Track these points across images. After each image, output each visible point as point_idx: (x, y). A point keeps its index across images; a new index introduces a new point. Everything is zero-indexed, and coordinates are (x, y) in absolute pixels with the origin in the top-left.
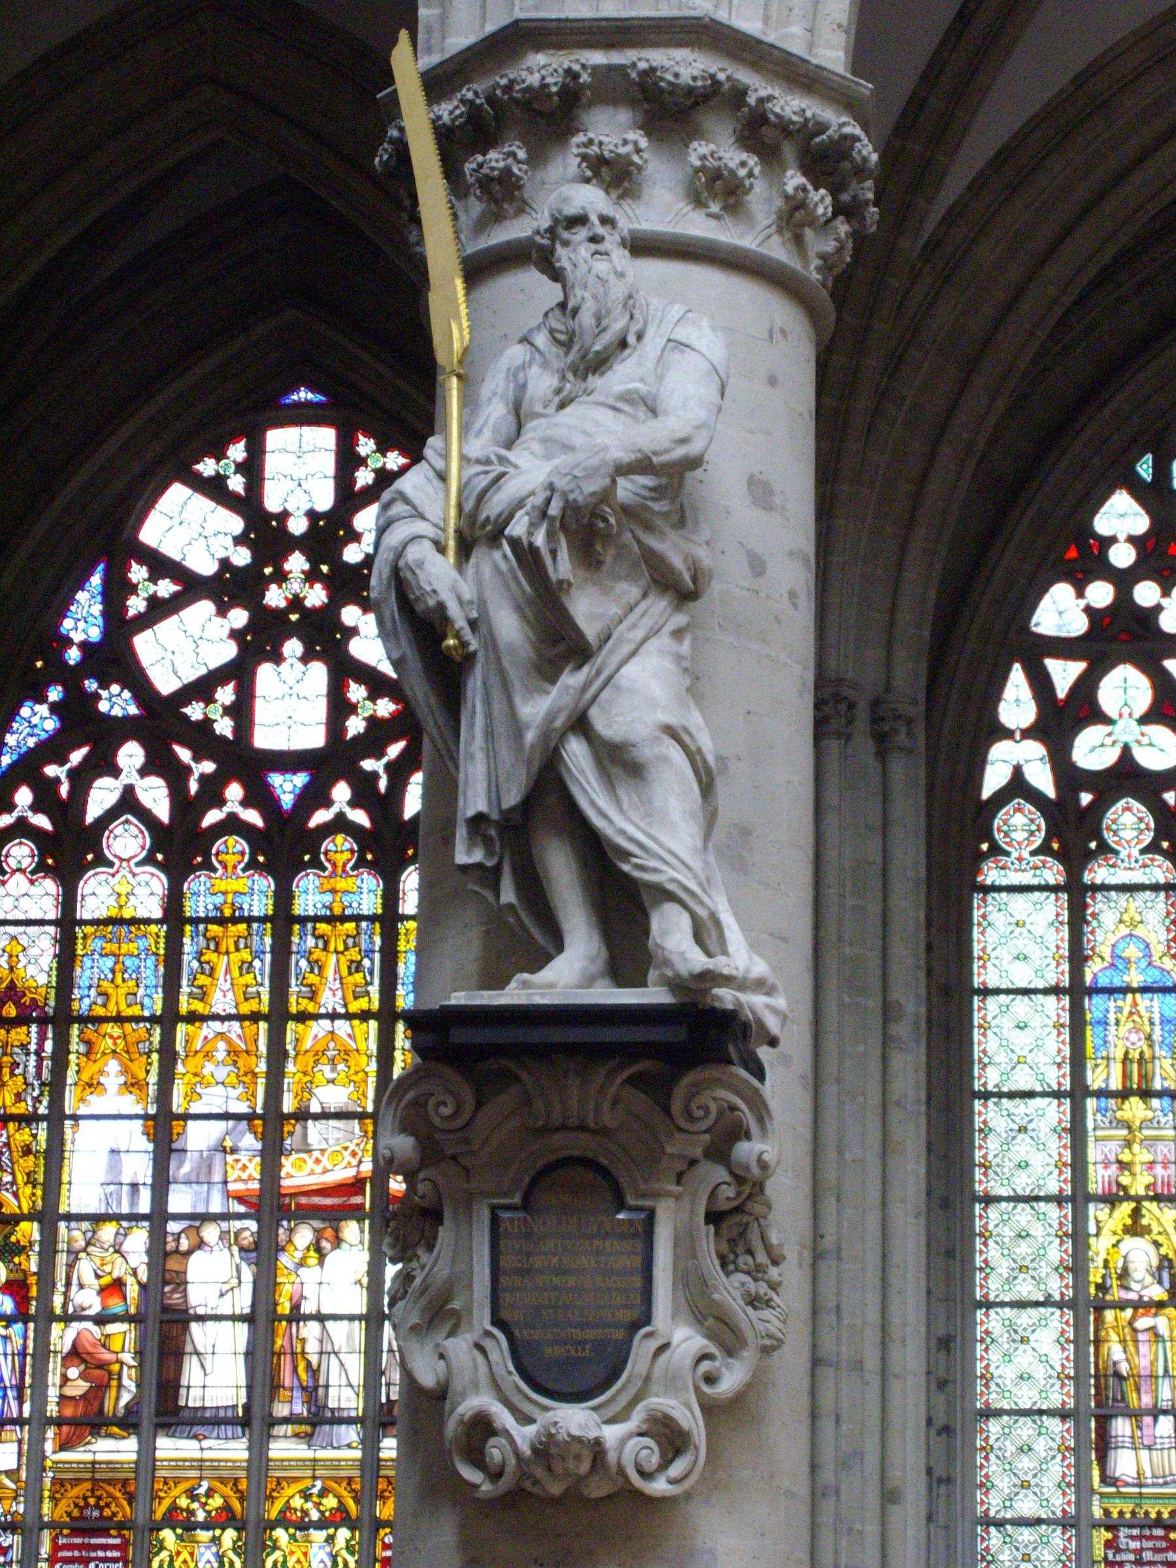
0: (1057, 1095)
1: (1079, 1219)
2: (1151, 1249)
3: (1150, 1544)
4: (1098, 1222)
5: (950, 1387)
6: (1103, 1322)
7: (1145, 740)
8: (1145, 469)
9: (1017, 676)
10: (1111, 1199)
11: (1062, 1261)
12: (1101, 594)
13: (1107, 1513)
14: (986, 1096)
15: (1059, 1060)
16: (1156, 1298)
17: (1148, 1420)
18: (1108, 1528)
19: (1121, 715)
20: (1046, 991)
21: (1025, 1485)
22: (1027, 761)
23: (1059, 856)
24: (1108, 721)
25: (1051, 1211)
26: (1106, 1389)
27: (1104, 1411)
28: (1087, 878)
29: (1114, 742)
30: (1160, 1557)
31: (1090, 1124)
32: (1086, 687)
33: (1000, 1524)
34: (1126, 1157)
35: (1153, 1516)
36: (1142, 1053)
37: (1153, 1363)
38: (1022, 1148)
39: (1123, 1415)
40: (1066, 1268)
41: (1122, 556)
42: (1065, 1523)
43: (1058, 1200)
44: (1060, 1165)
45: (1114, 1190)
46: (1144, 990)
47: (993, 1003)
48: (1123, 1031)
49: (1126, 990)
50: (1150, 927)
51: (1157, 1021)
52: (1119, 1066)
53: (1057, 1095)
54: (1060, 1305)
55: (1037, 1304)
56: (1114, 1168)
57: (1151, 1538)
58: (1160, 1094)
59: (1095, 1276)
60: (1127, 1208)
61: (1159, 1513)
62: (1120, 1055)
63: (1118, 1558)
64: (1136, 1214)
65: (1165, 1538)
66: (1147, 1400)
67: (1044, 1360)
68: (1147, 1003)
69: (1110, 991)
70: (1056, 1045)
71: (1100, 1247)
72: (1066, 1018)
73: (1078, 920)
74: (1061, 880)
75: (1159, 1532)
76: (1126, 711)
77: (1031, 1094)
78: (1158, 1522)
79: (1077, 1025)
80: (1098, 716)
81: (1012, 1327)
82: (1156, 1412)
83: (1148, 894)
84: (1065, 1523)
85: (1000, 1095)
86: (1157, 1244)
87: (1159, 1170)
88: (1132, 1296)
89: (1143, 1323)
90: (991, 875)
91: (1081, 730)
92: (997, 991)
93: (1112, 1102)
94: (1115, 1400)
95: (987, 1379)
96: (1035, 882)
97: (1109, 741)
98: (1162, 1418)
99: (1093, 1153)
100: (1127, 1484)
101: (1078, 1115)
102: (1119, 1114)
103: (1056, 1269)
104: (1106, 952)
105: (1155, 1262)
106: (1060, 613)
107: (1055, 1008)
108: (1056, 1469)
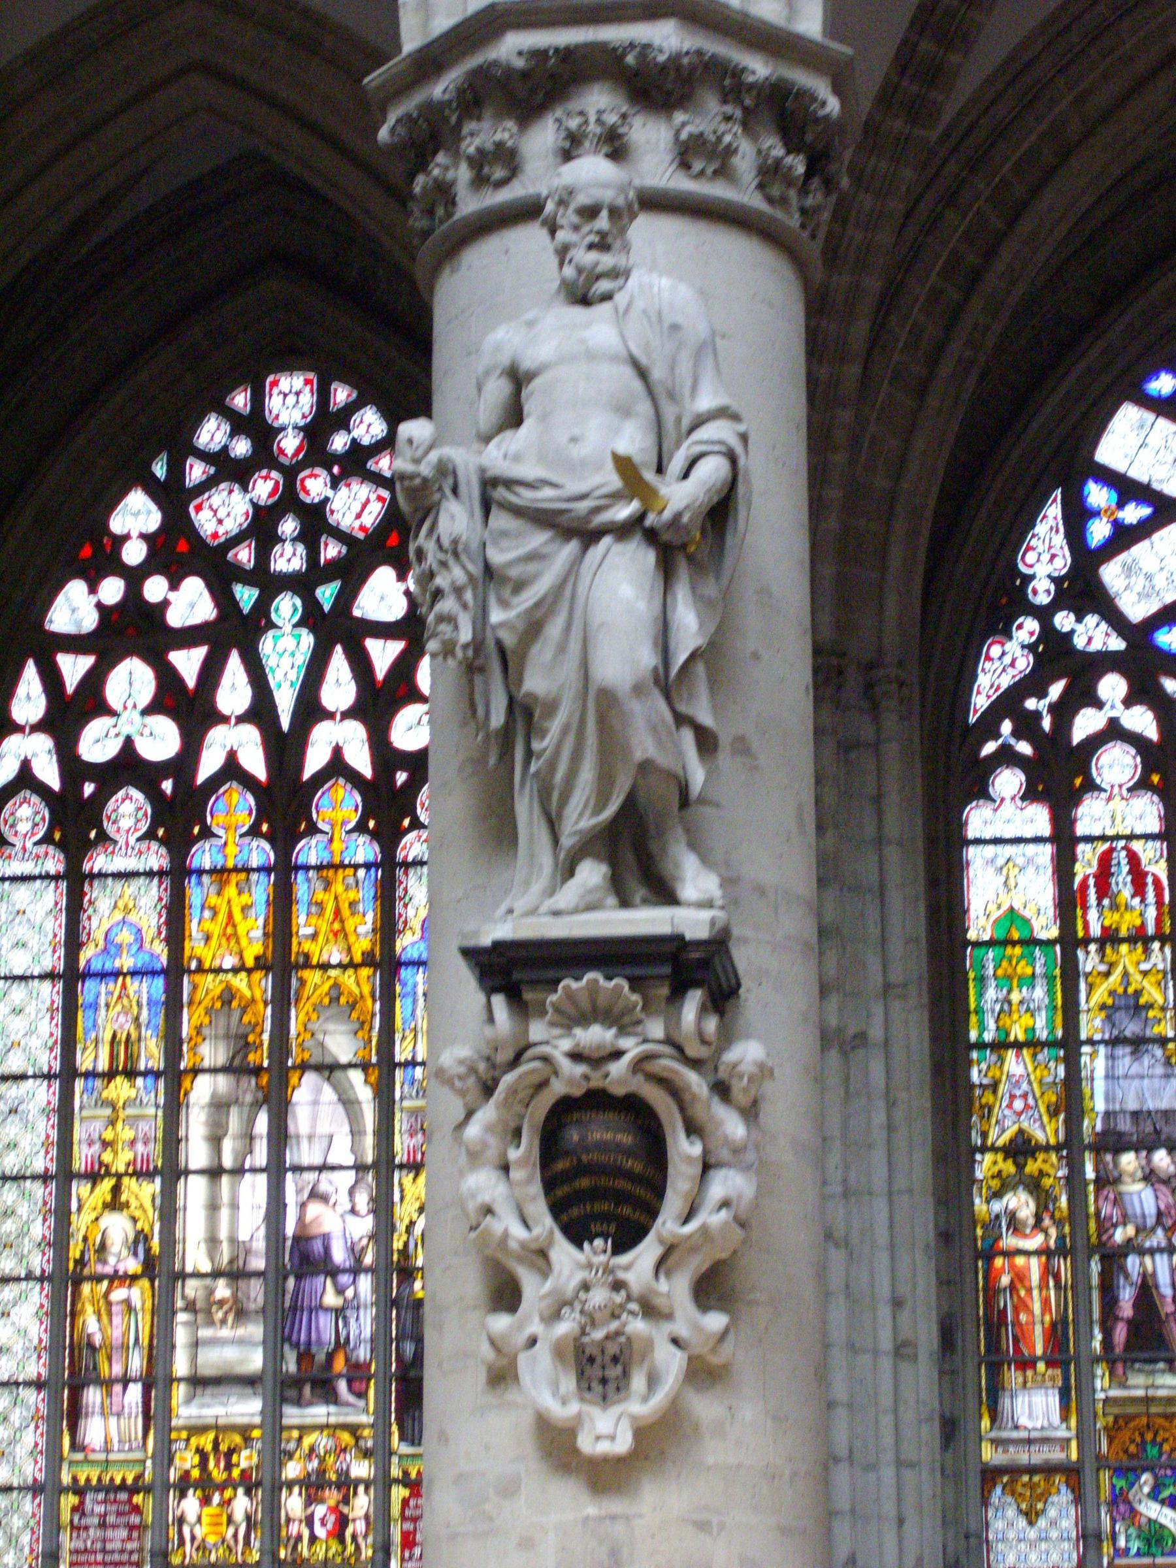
1: (64, 1196)
3: (114, 1508)
4: (79, 1200)
6: (80, 1295)
8: (160, 470)
10: (93, 1177)
11: (44, 1237)
12: (112, 590)
13: (75, 1479)
16: (130, 1272)
17: (118, 1388)
18: (76, 1493)
19: (125, 708)
20: (42, 977)
23: (62, 846)
25: (37, 1190)
27: (77, 1381)
28: (86, 867)
29: (117, 735)
30: (123, 1520)
32: (94, 681)
34: (109, 1135)
35: (118, 1481)
36: (129, 1036)
40: (49, 1244)
41: (134, 553)
43: (45, 1178)
44: (47, 1145)
45: (96, 1167)
46: (134, 973)
48: (112, 1013)
49: (116, 974)
50: (142, 912)
51: (144, 1001)
53: (48, 1076)
54: (41, 1279)
55: (18, 1279)
56: (97, 1147)
58: (146, 1074)
59: (75, 1252)
60: (107, 1184)
61: (124, 1480)
62: (108, 1036)
63: (83, 1522)
64: (116, 1190)
66: (117, 1369)
68: (136, 984)
69: (103, 975)
70: (48, 1029)
71: (80, 1223)
72: (58, 1001)
73: (75, 908)
74: (61, 868)
75: (123, 1496)
77: (23, 1077)
78: (123, 1486)
79: (70, 1010)
80: (102, 708)
82: (126, 1381)
83: (142, 880)
84: (35, 1489)
86: (135, 1220)
87: (140, 1147)
88: (108, 1270)
89: (119, 1294)
91: (88, 723)
93: (98, 1083)
96: (36, 872)
98: (131, 1386)
99: (79, 1132)
100: (93, 1451)
101: (66, 1096)
102: (105, 1094)
104: (99, 935)
105: (131, 1236)
106: (73, 611)
107: (49, 992)
108: (29, 1438)
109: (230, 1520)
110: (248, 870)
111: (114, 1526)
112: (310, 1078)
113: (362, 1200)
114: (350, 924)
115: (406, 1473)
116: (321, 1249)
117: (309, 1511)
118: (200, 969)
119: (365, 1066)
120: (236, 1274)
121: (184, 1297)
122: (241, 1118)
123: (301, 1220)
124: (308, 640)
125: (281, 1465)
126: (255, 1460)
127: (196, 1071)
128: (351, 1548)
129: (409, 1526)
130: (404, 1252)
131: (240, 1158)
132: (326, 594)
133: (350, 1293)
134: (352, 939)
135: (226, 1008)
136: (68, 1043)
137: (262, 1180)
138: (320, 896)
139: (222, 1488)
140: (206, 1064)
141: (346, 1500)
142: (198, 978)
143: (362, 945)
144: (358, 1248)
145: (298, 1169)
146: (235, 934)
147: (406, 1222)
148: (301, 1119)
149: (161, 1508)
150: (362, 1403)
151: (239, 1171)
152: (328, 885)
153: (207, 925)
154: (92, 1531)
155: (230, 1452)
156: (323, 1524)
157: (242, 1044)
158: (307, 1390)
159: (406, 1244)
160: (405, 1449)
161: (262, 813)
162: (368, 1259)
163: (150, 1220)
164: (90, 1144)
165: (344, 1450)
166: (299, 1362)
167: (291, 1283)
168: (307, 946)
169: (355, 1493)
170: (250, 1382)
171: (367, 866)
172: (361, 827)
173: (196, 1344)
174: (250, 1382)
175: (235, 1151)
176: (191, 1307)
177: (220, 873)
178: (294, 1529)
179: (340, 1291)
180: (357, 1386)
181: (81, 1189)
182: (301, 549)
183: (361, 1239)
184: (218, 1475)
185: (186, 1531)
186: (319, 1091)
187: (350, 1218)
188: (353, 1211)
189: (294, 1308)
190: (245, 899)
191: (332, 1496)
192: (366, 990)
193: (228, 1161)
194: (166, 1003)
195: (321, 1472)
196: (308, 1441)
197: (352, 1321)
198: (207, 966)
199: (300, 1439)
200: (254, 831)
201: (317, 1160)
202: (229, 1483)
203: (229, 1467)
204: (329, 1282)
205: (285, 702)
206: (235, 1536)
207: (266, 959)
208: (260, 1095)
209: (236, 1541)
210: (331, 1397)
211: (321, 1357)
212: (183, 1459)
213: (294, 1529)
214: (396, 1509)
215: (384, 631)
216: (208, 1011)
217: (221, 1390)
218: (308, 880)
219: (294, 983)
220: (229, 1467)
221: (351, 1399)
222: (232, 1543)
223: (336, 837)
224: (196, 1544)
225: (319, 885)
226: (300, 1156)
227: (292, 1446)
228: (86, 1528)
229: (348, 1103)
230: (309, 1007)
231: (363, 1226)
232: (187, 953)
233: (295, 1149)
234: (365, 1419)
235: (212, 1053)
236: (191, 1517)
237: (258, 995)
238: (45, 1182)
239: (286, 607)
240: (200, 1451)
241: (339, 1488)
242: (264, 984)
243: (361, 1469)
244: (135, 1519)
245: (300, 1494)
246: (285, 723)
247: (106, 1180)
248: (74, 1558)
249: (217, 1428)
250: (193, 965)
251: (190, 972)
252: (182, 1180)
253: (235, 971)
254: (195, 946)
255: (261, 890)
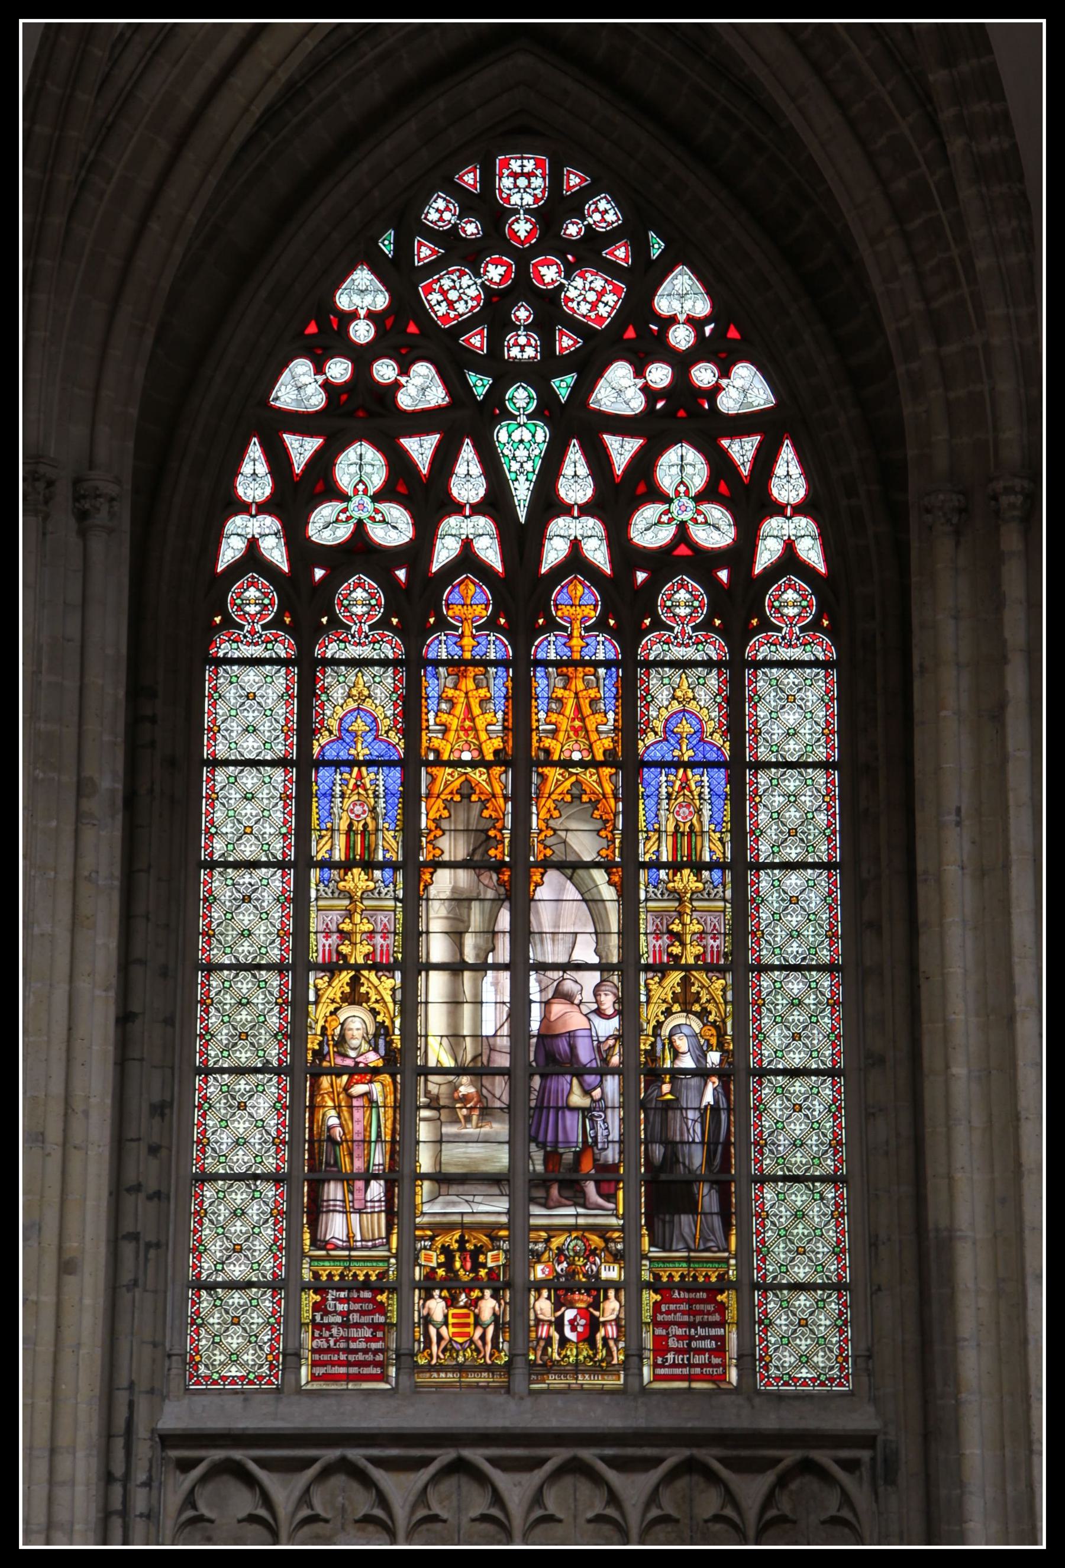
0: (281, 865)
1: (300, 986)
2: (368, 1018)
3: (357, 1306)
4: (317, 990)
5: (164, 1153)
6: (319, 1089)
7: (378, 517)
8: (387, 245)
9: (255, 450)
10: (331, 969)
13: (316, 1275)
14: (212, 865)
15: (284, 830)
17: (360, 1184)
21: (237, 1249)
22: (262, 536)
24: (345, 498)
25: (274, 980)
26: (320, 1153)
28: (318, 652)
29: (349, 518)
30: (366, 1319)
31: (313, 894)
33: (211, 1287)
34: (347, 927)
35: (361, 1278)
36: (365, 825)
37: (367, 1128)
38: (246, 917)
39: (336, 1180)
40: (286, 1036)
41: (362, 332)
42: (275, 1286)
43: (279, 968)
46: (369, 763)
47: (221, 775)
48: (347, 803)
49: (352, 763)
52: (343, 838)
53: (281, 865)
54: (277, 1072)
55: (256, 1071)
56: (334, 938)
57: (359, 1300)
59: (313, 1044)
60: (346, 976)
61: (367, 1275)
62: (344, 826)
63: (325, 1321)
65: (372, 1300)
66: (359, 1165)
67: (260, 1125)
68: (372, 776)
69: (337, 764)
71: (319, 1014)
75: (367, 1295)
76: (361, 487)
77: (254, 865)
78: (366, 1285)
81: (229, 1093)
82: (368, 1177)
84: (275, 1286)
85: (226, 865)
86: (374, 1013)
87: (379, 940)
88: (349, 1063)
89: (359, 1089)
90: (224, 649)
92: (227, 763)
94: (328, 1164)
95: (203, 1144)
96: (267, 655)
97: (343, 517)
98: (373, 1183)
99: (315, 923)
100: (336, 1248)
101: (302, 885)
103: (276, 1035)
105: (372, 1030)
109: (477, 1322)
110: (486, 663)
111: (358, 1325)
112: (552, 875)
113: (608, 1003)
114: (591, 724)
115: (657, 1277)
116: (567, 1048)
117: (559, 1313)
118: (439, 763)
119: (607, 866)
120: (479, 1071)
121: (427, 1093)
122: (482, 912)
123: (545, 1019)
124: (542, 434)
125: (531, 1266)
126: (502, 1260)
127: (437, 865)
128: (602, 1354)
129: (660, 1331)
130: (651, 1053)
131: (482, 955)
132: (563, 386)
133: (597, 1093)
134: (594, 736)
135: (465, 801)
136: (302, 832)
137: (505, 977)
138: (560, 693)
139: (468, 1289)
140: (446, 857)
141: (596, 1305)
142: (434, 770)
143: (603, 744)
144: (604, 1047)
145: (542, 967)
146: (474, 728)
147: (653, 1023)
148: (543, 917)
149: (405, 1308)
150: (612, 1206)
151: (481, 967)
152: (568, 680)
153: (444, 717)
154: (334, 1331)
155: (479, 1250)
156: (573, 1329)
157: (483, 838)
158: (555, 1191)
159: (653, 1045)
160: (655, 1252)
161: (500, 605)
162: (615, 1060)
163: (390, 1013)
164: (327, 935)
165: (593, 1252)
166: (546, 1162)
167: (537, 1081)
168: (547, 742)
169: (606, 1298)
170: (495, 1180)
171: (607, 664)
172: (600, 625)
173: (439, 1141)
174: (495, 1180)
175: (476, 947)
176: (434, 1104)
177: (457, 665)
178: (543, 1331)
179: (587, 1092)
180: (605, 1187)
181: (316, 980)
182: (535, 337)
183: (608, 1038)
184: (465, 1276)
185: (433, 1331)
186: (562, 889)
187: (597, 1020)
188: (599, 1012)
189: (540, 1107)
190: (483, 692)
191: (582, 1300)
192: (608, 788)
193: (470, 957)
194: (403, 795)
195: (571, 1274)
196: (555, 1243)
197: (600, 1121)
198: (445, 757)
199: (547, 1241)
200: (491, 625)
201: (562, 959)
202: (476, 1284)
203: (477, 1266)
204: (575, 1081)
205: (522, 491)
206: (483, 1337)
207: (506, 753)
208: (502, 890)
209: (484, 1344)
210: (580, 1199)
211: (568, 1157)
212: (428, 1259)
213: (543, 1331)
214: (647, 1315)
215: (622, 425)
216: (447, 804)
217: (466, 1188)
218: (547, 676)
219: (535, 778)
220: (477, 1266)
221: (601, 1201)
222: (480, 1343)
223: (576, 633)
224: (443, 1344)
225: (559, 682)
226: (543, 954)
227: (540, 1247)
228: (329, 1327)
229: (591, 901)
230: (550, 804)
231: (607, 1028)
232: (425, 744)
233: (538, 947)
234: (613, 1221)
235: (452, 847)
236: (438, 1316)
237: (498, 790)
238: (280, 972)
239: (521, 397)
240: (445, 1250)
241: (588, 1291)
242: (501, 780)
243: (611, 1273)
244: (379, 1319)
245: (549, 1298)
246: (522, 514)
247: (344, 973)
248: (317, 1357)
249: (462, 1226)
250: (431, 757)
251: (429, 764)
252: (423, 974)
253: (473, 764)
254: (432, 740)
255: (499, 683)
